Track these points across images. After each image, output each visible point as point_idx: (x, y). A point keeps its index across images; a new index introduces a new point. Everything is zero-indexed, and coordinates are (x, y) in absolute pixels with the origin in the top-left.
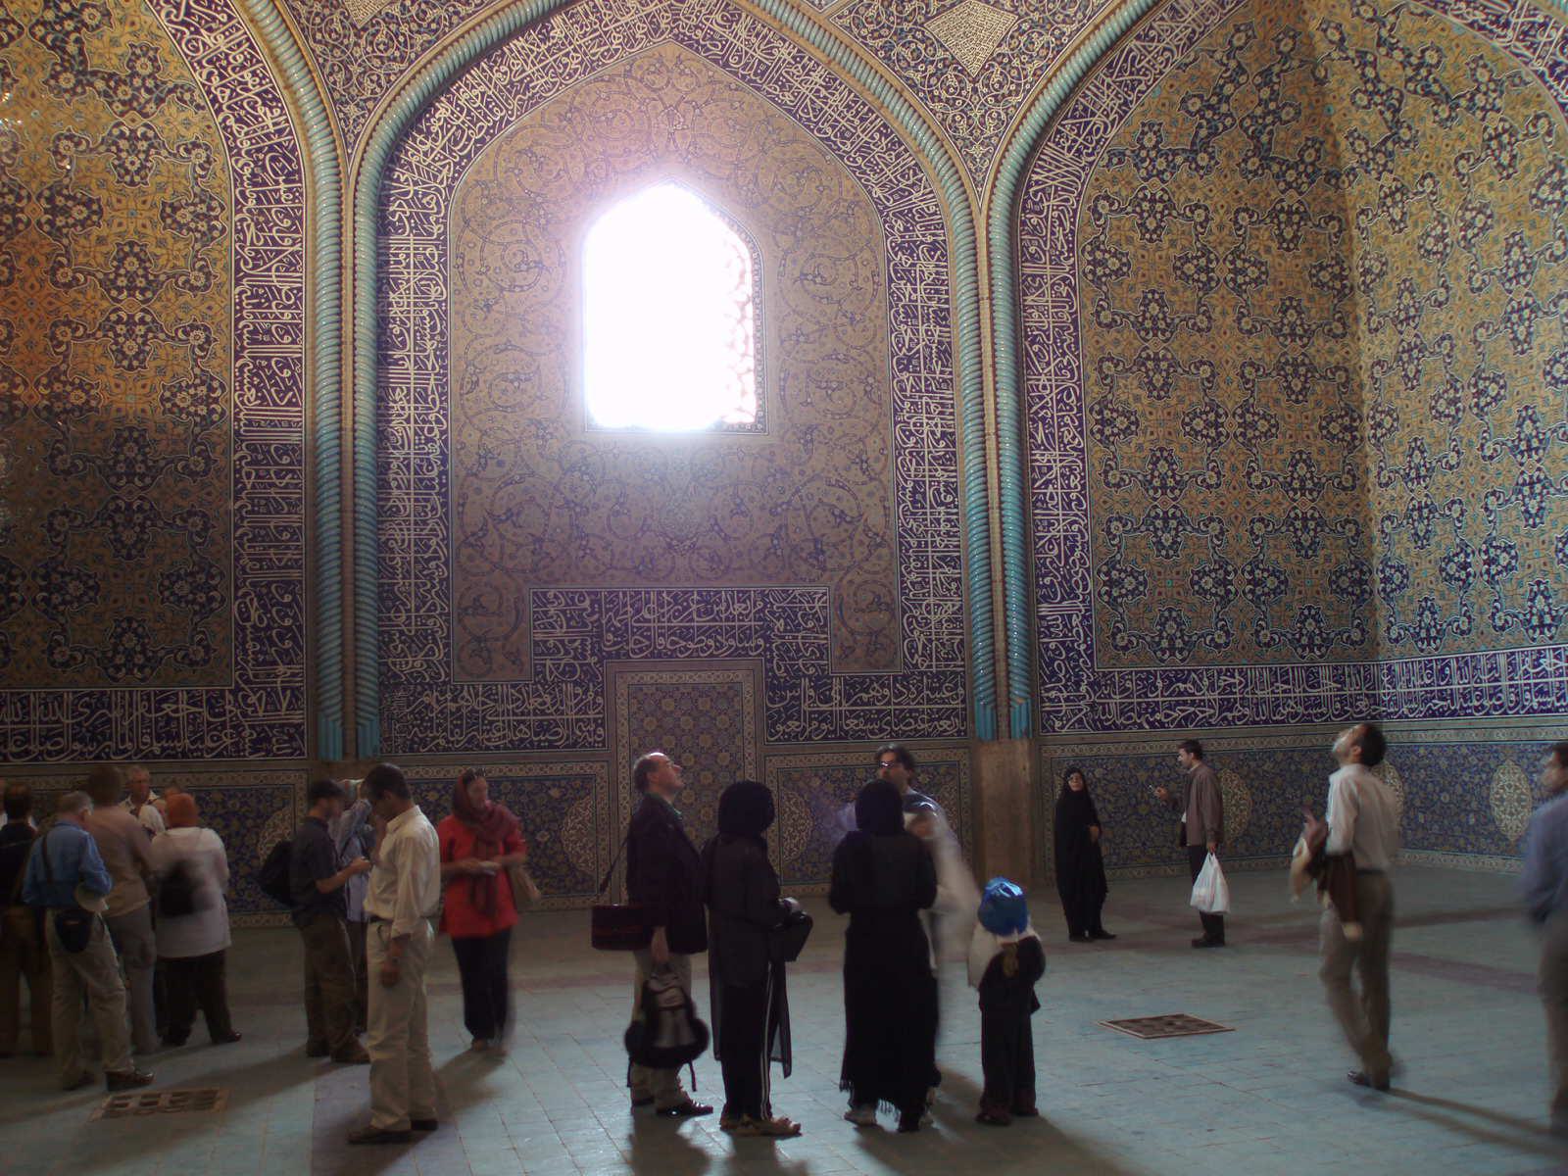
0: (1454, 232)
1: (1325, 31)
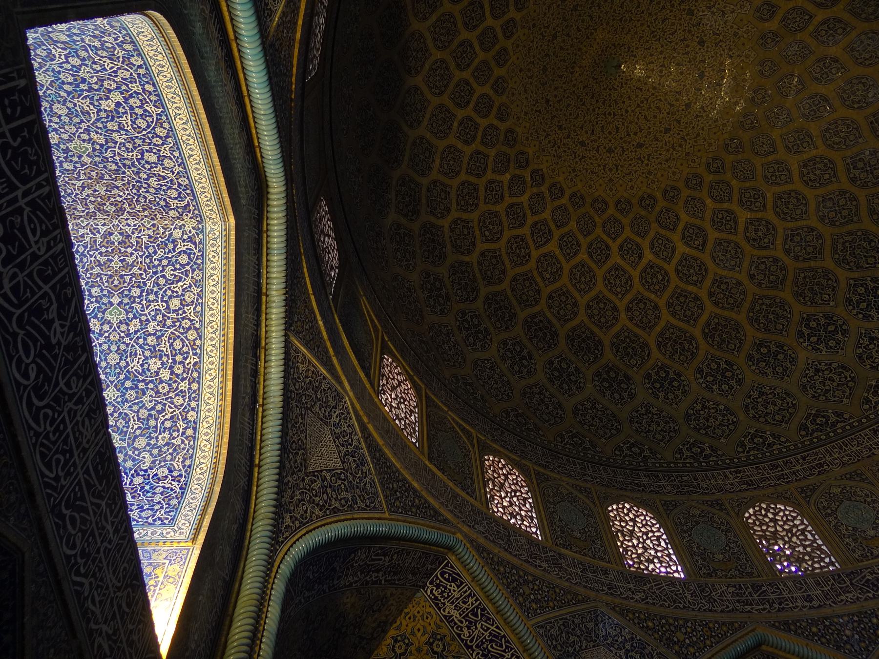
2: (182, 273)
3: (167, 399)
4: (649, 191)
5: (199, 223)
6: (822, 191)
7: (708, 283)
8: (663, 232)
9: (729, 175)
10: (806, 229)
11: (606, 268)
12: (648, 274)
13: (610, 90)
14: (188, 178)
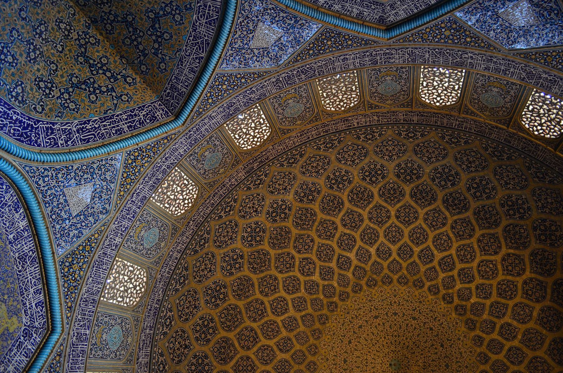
0: (38, 41)
1: (133, 79)
4: (371, 290)
6: (277, 295)
7: (337, 236)
8: (363, 265)
9: (325, 302)
10: (284, 271)
11: (401, 242)
12: (373, 239)
13: (395, 351)
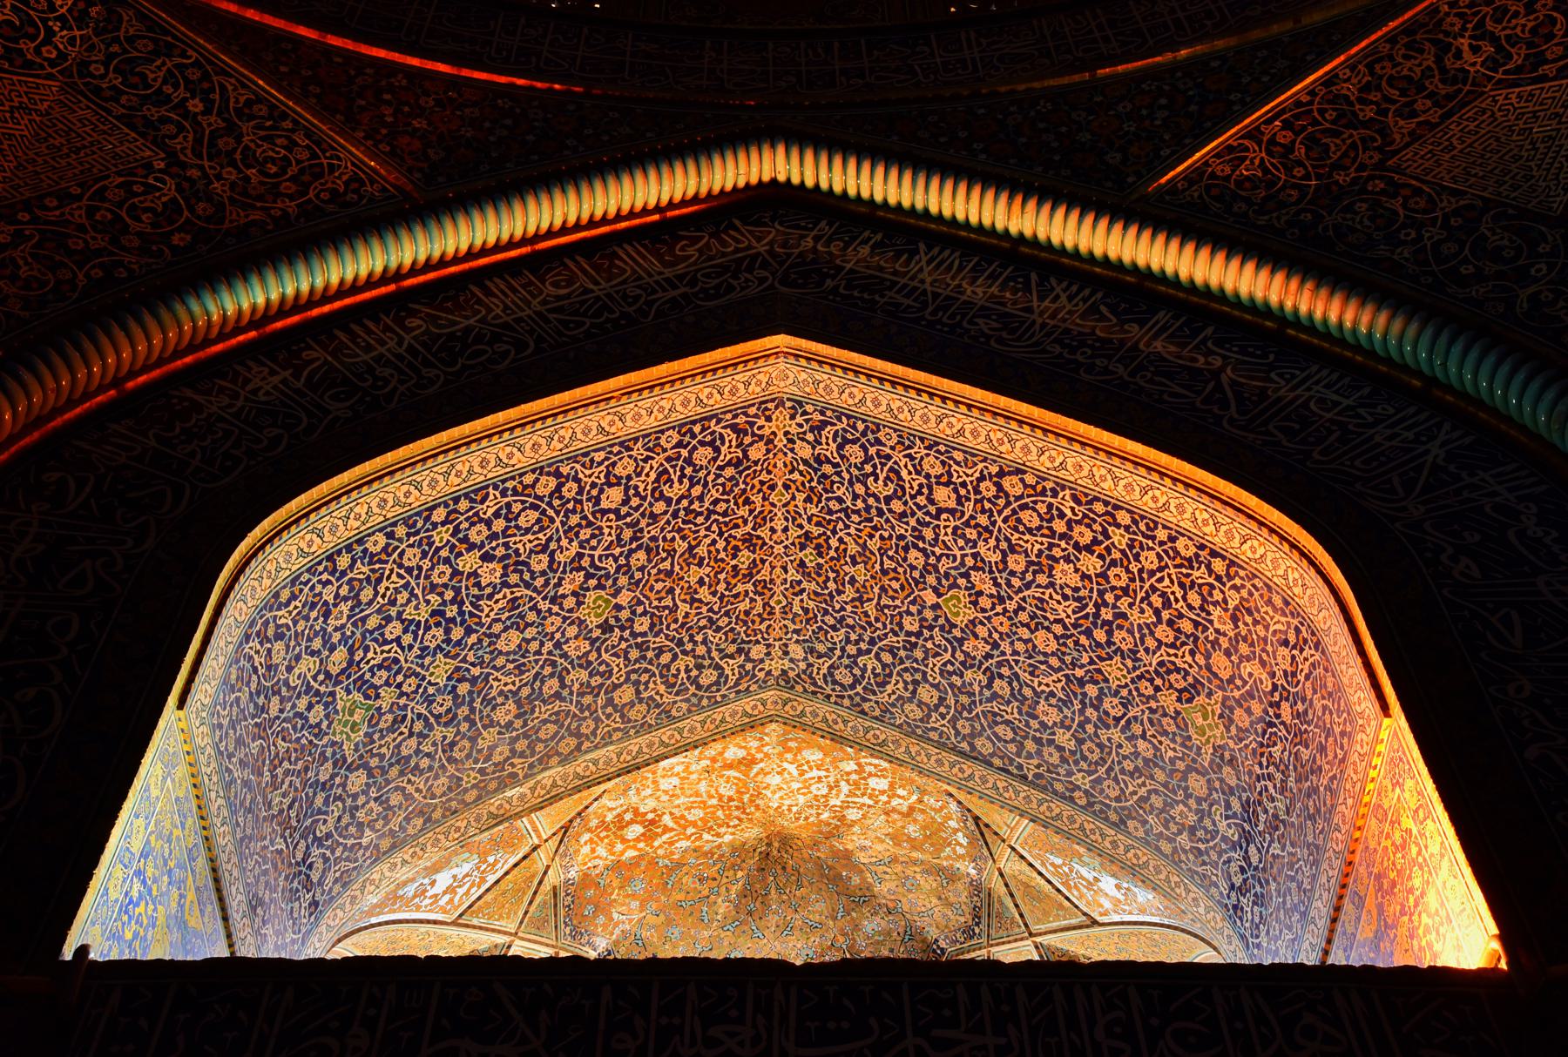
2: (883, 465)
3: (1142, 580)
5: (781, 403)
14: (662, 432)
